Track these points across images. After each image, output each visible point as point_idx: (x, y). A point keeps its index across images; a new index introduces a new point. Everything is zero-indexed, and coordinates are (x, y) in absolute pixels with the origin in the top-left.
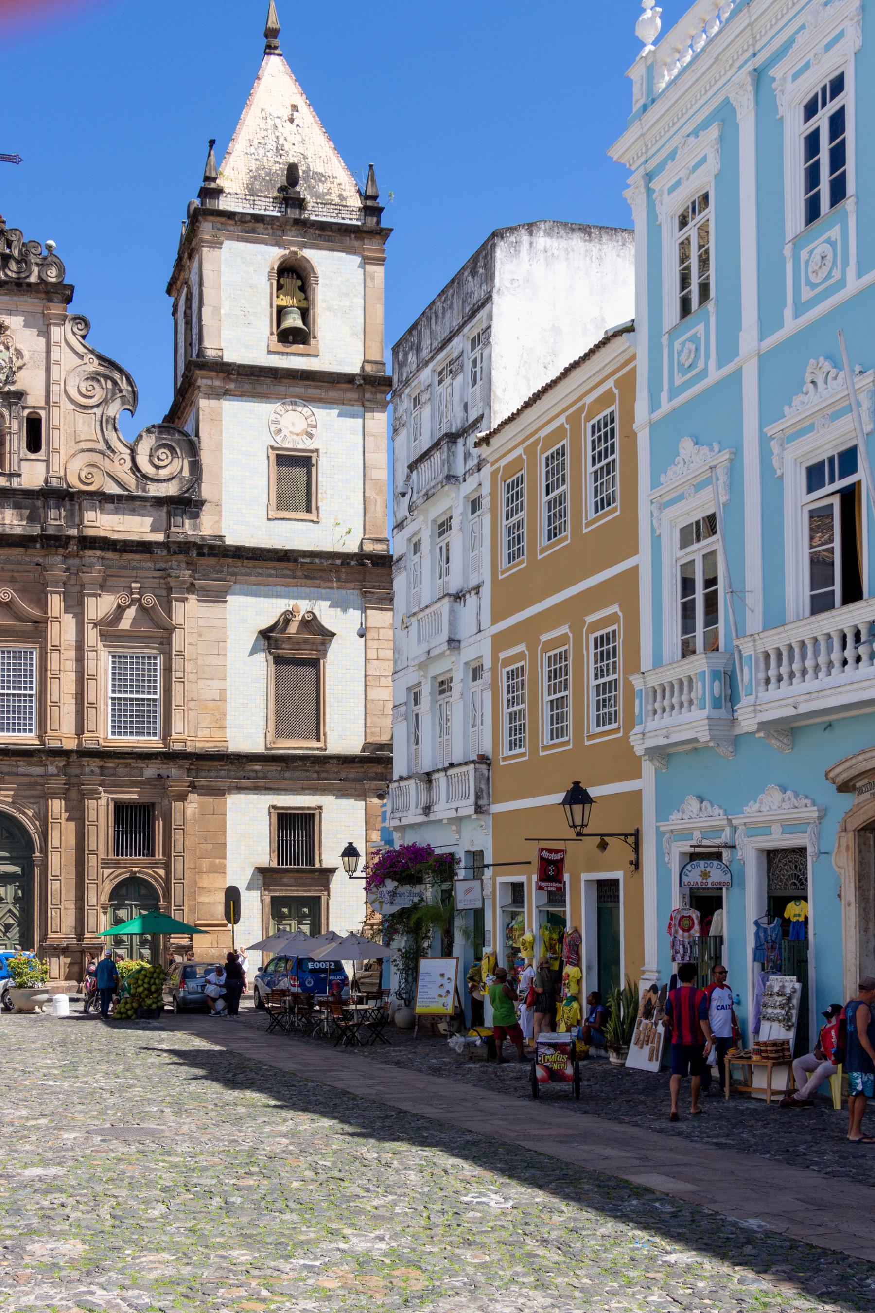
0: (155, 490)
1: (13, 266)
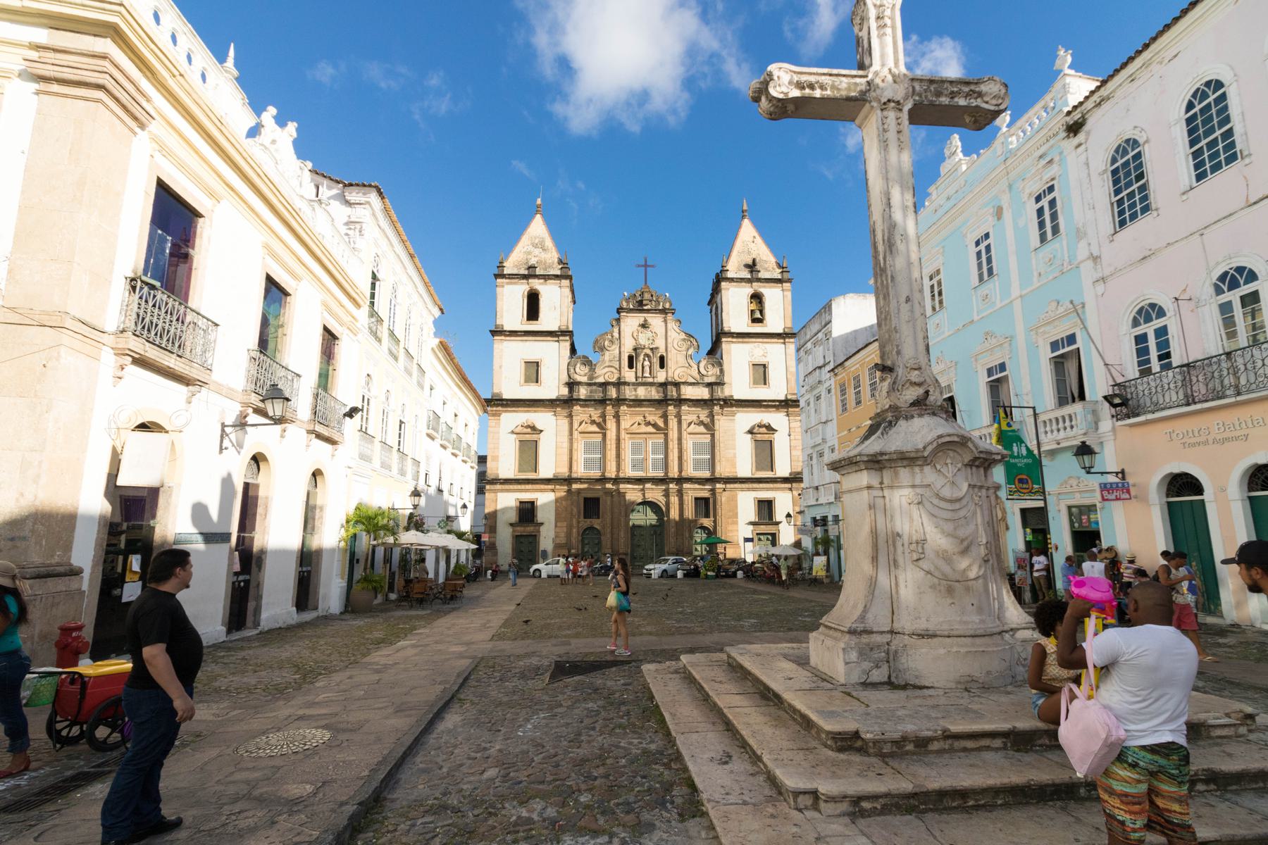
0: (707, 380)
1: (653, 303)
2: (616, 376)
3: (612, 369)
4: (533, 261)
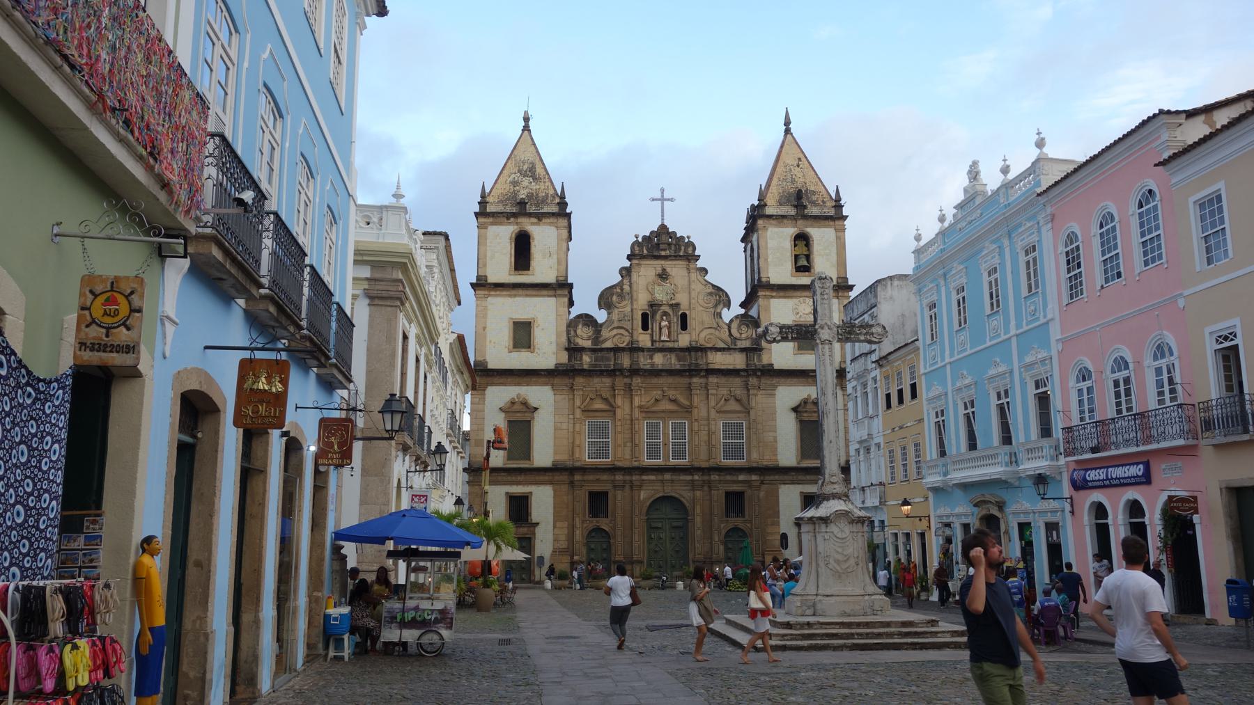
1: (673, 248)
2: (627, 339)
3: (622, 331)
4: (523, 194)
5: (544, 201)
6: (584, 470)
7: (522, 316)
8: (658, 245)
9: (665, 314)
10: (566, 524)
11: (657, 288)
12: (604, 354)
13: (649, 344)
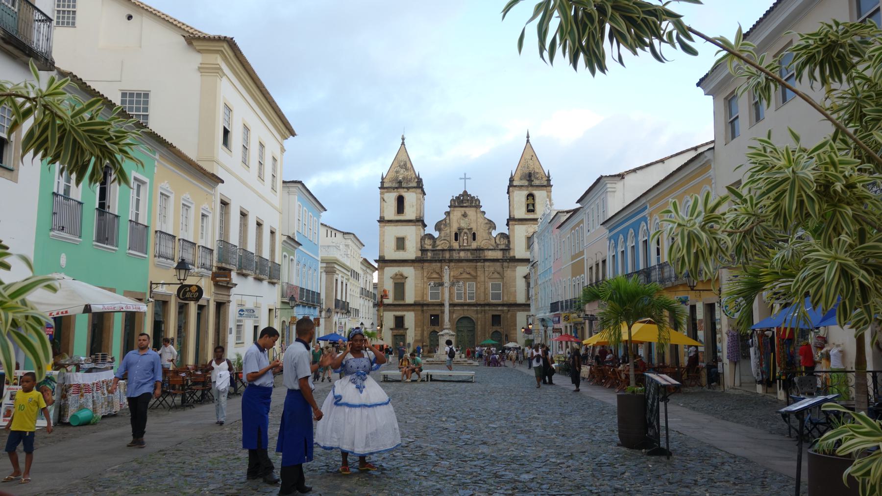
2: (448, 245)
3: (446, 241)
5: (410, 181)
6: (428, 305)
7: (401, 235)
8: (462, 200)
9: (466, 233)
10: (420, 329)
11: (462, 221)
12: (438, 252)
13: (458, 247)
